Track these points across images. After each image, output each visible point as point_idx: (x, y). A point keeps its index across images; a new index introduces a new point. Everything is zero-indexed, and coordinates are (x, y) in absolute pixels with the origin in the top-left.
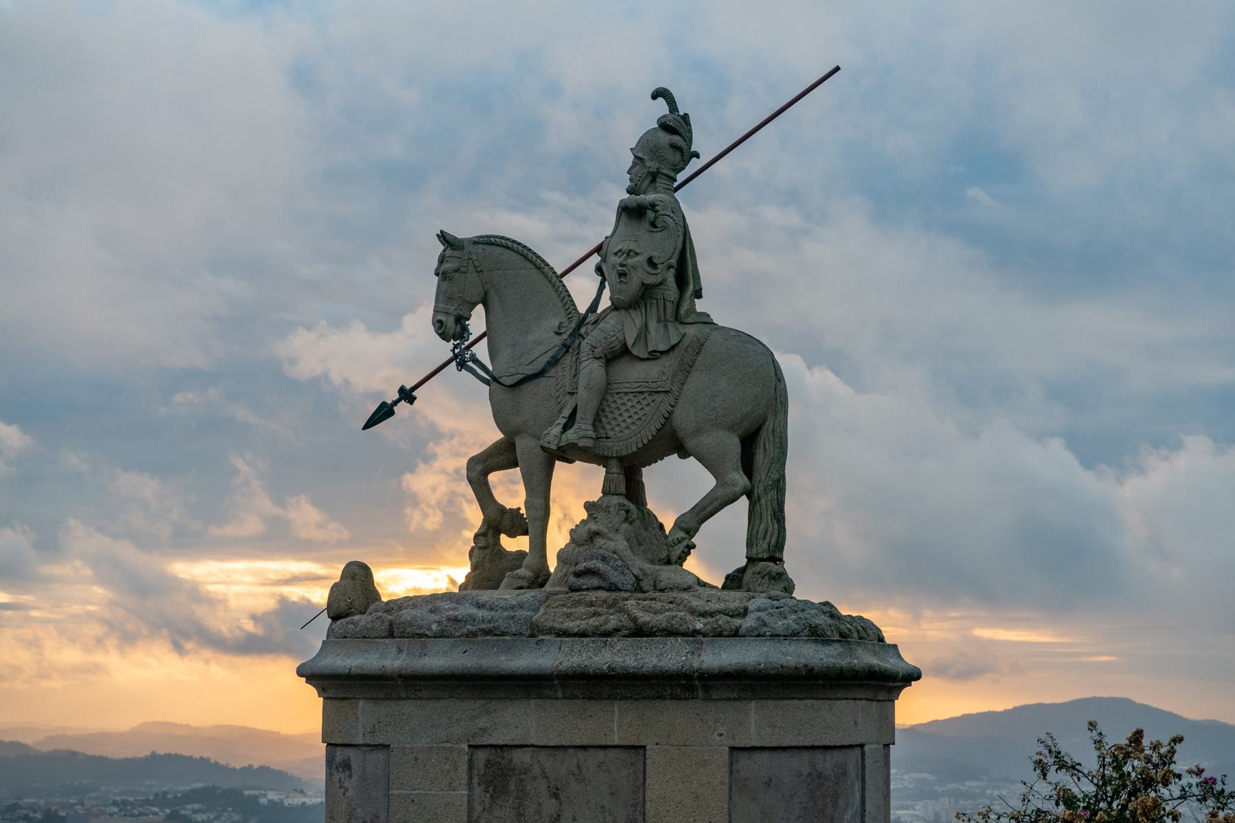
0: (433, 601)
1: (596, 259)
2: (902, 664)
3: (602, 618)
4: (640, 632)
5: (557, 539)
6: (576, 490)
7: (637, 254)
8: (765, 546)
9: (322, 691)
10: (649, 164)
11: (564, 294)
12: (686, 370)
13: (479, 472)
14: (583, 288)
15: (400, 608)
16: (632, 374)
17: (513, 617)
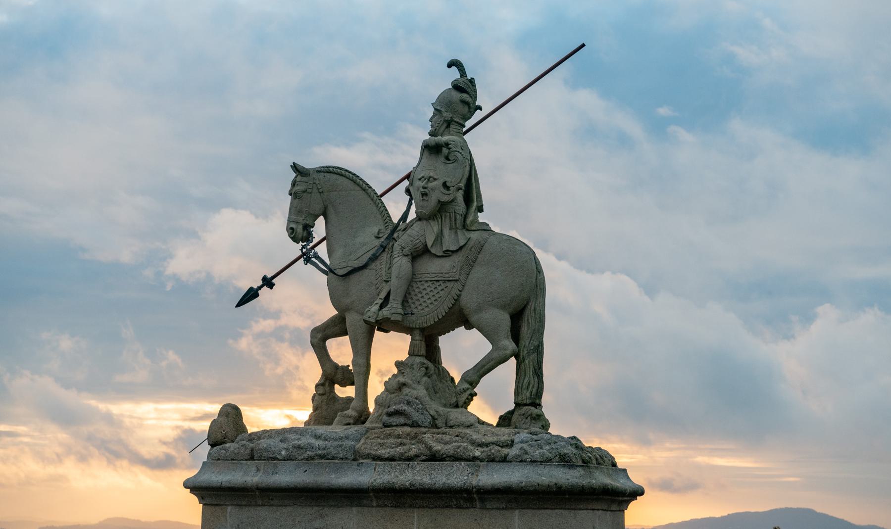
0: (282, 434)
1: (406, 183)
2: (629, 484)
3: (406, 448)
4: (434, 457)
5: (376, 387)
6: (391, 350)
7: (435, 179)
8: (528, 394)
9: (201, 499)
10: (445, 114)
11: (382, 208)
12: (471, 264)
13: (320, 338)
14: (396, 206)
15: (259, 438)
16: (431, 267)
17: (341, 446)
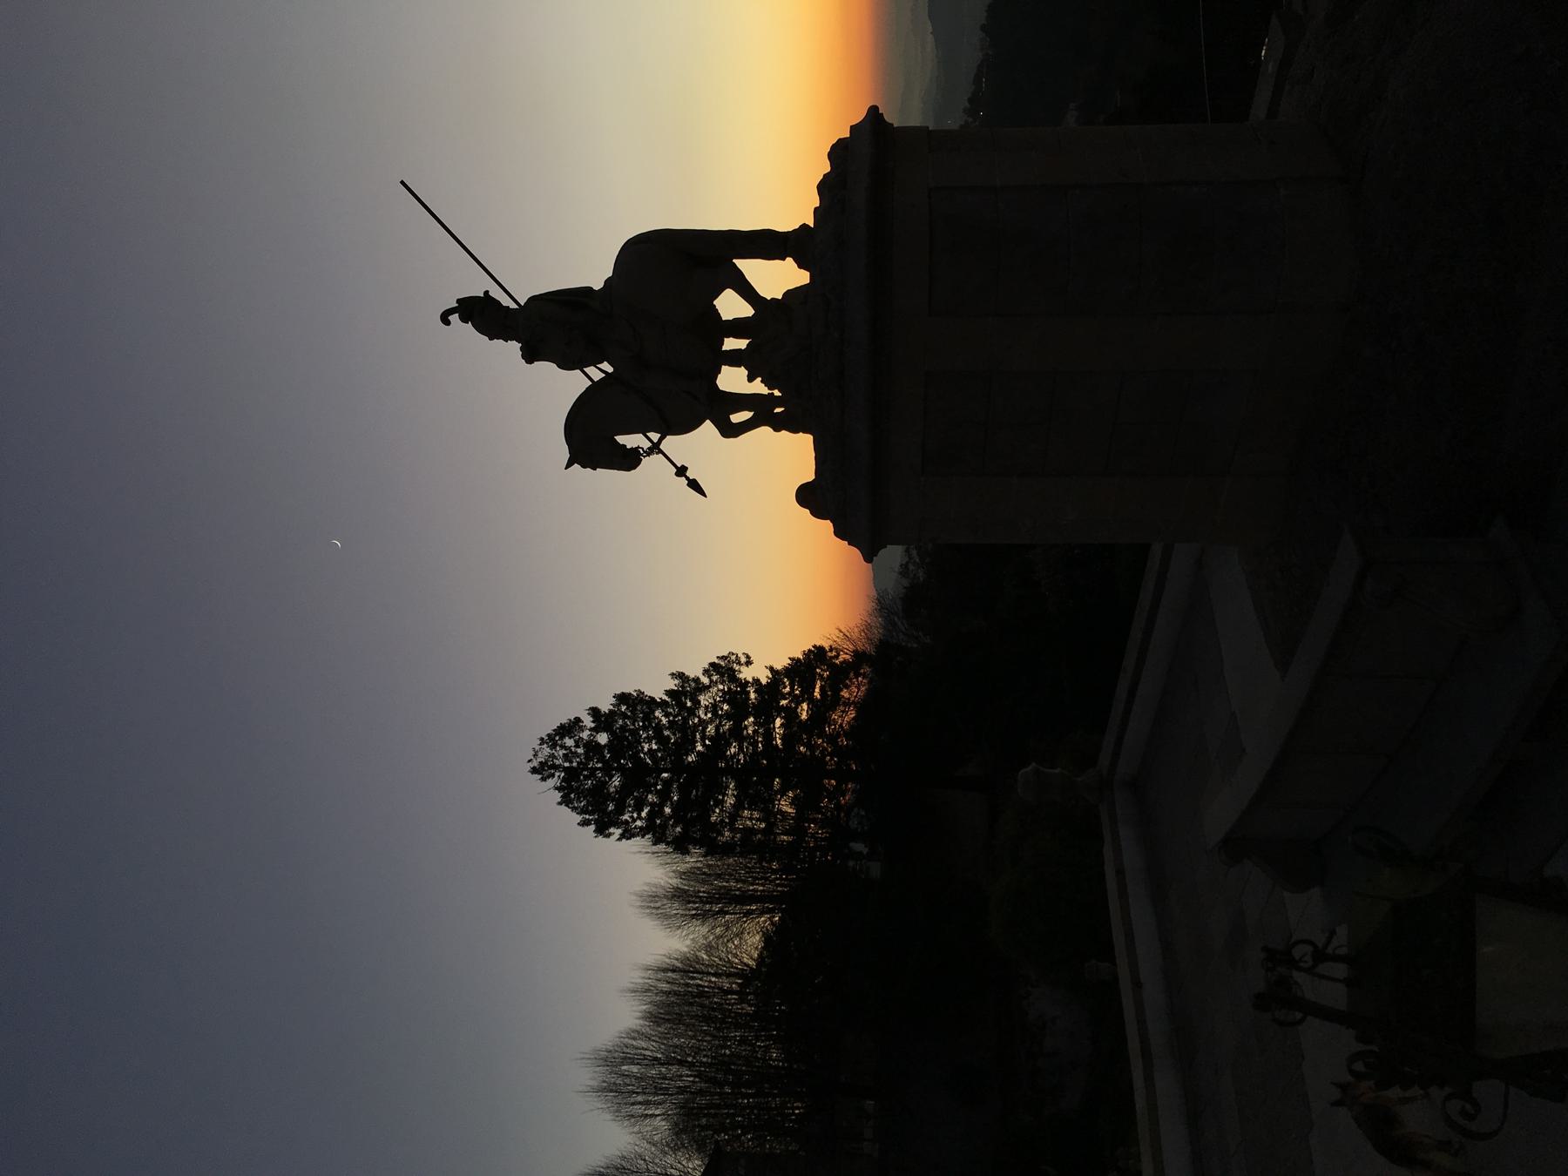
13: (730, 431)
14: (597, 375)
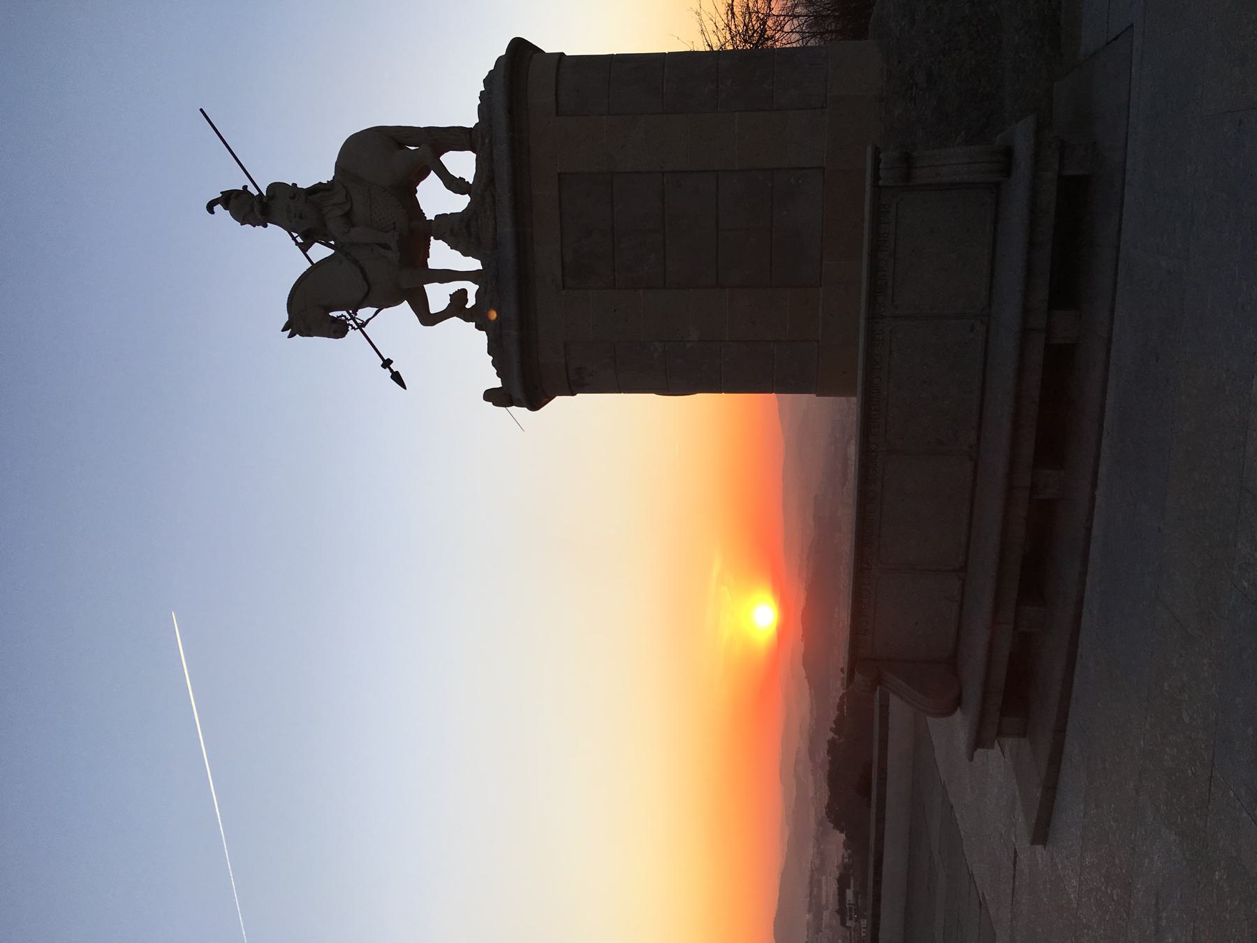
13: (428, 319)
14: (320, 252)
